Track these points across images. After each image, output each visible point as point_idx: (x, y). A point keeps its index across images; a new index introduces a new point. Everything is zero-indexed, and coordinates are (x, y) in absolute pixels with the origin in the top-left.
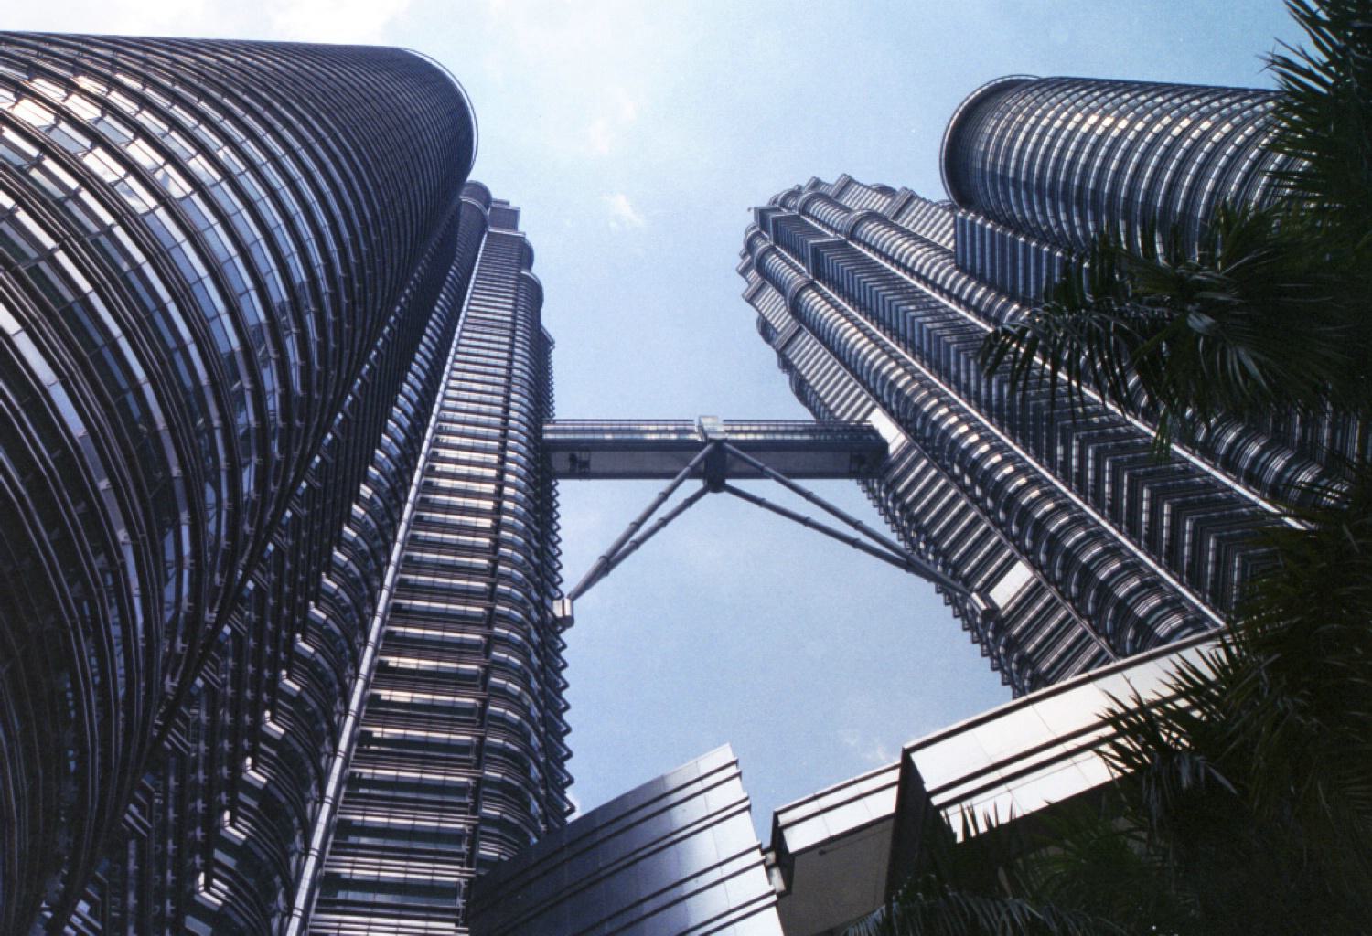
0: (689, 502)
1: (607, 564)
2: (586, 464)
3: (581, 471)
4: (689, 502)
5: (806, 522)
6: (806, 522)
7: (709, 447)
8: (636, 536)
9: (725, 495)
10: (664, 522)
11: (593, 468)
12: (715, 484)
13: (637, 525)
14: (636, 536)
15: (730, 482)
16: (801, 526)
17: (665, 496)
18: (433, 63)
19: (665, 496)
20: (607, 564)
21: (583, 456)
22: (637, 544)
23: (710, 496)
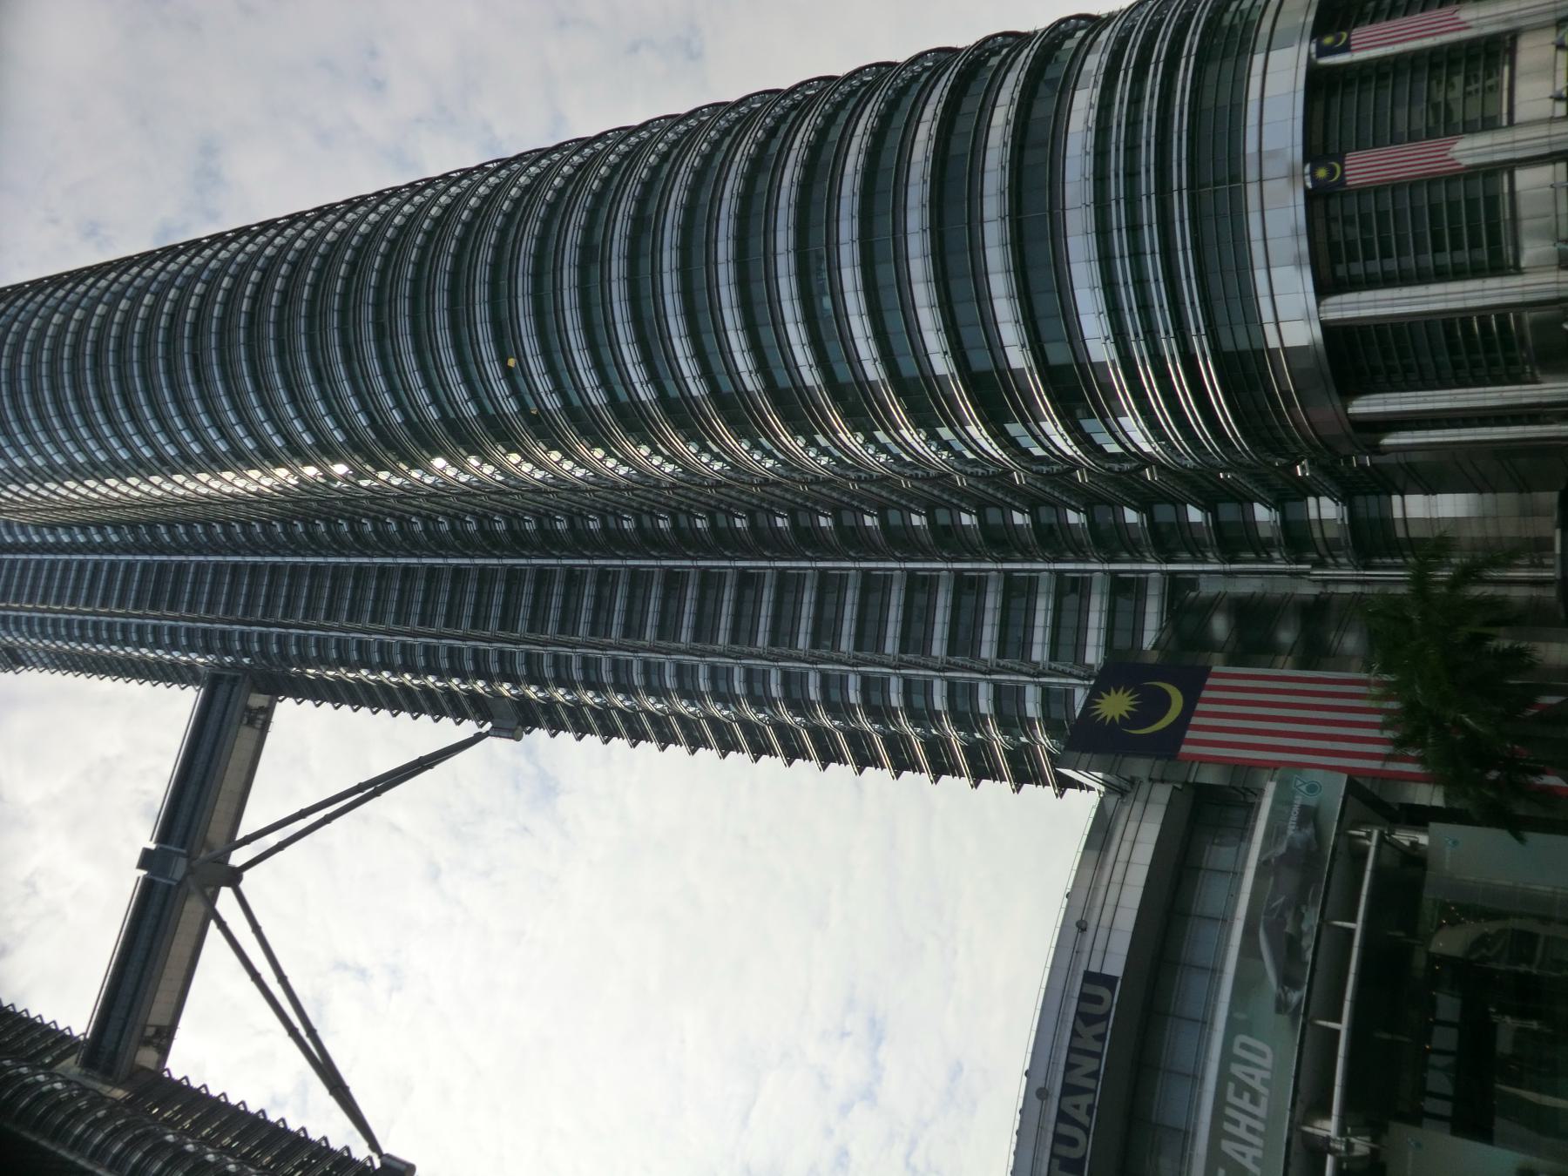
0: (256, 929)
4: (256, 929)
8: (303, 1032)
10: (282, 979)
12: (233, 878)
16: (327, 826)
23: (243, 886)
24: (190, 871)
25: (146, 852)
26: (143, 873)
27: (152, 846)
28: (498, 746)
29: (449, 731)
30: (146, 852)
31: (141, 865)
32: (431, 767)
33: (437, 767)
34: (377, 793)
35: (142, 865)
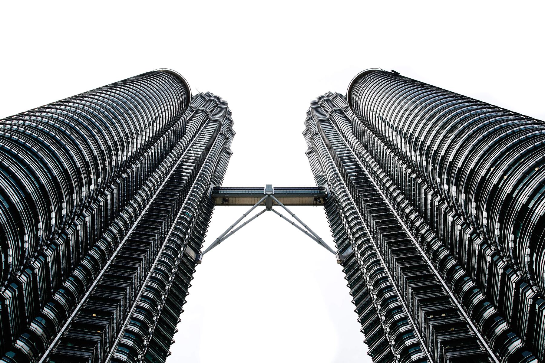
0: (257, 216)
1: (219, 241)
2: (228, 201)
3: (226, 202)
4: (257, 216)
5: (293, 224)
6: (293, 224)
7: (266, 196)
9: (271, 211)
10: (245, 224)
11: (230, 202)
12: (269, 208)
13: (232, 227)
14: (232, 230)
15: (274, 208)
17: (245, 215)
18: (171, 71)
19: (245, 215)
20: (219, 241)
21: (227, 199)
22: (233, 233)
23: (267, 212)
24: (269, 195)
25: (271, 186)
26: (265, 187)
27: (273, 187)
28: (334, 258)
29: (332, 245)
30: (271, 186)
31: (267, 186)
32: (319, 243)
33: (320, 245)
34: (306, 233)
35: (267, 186)
